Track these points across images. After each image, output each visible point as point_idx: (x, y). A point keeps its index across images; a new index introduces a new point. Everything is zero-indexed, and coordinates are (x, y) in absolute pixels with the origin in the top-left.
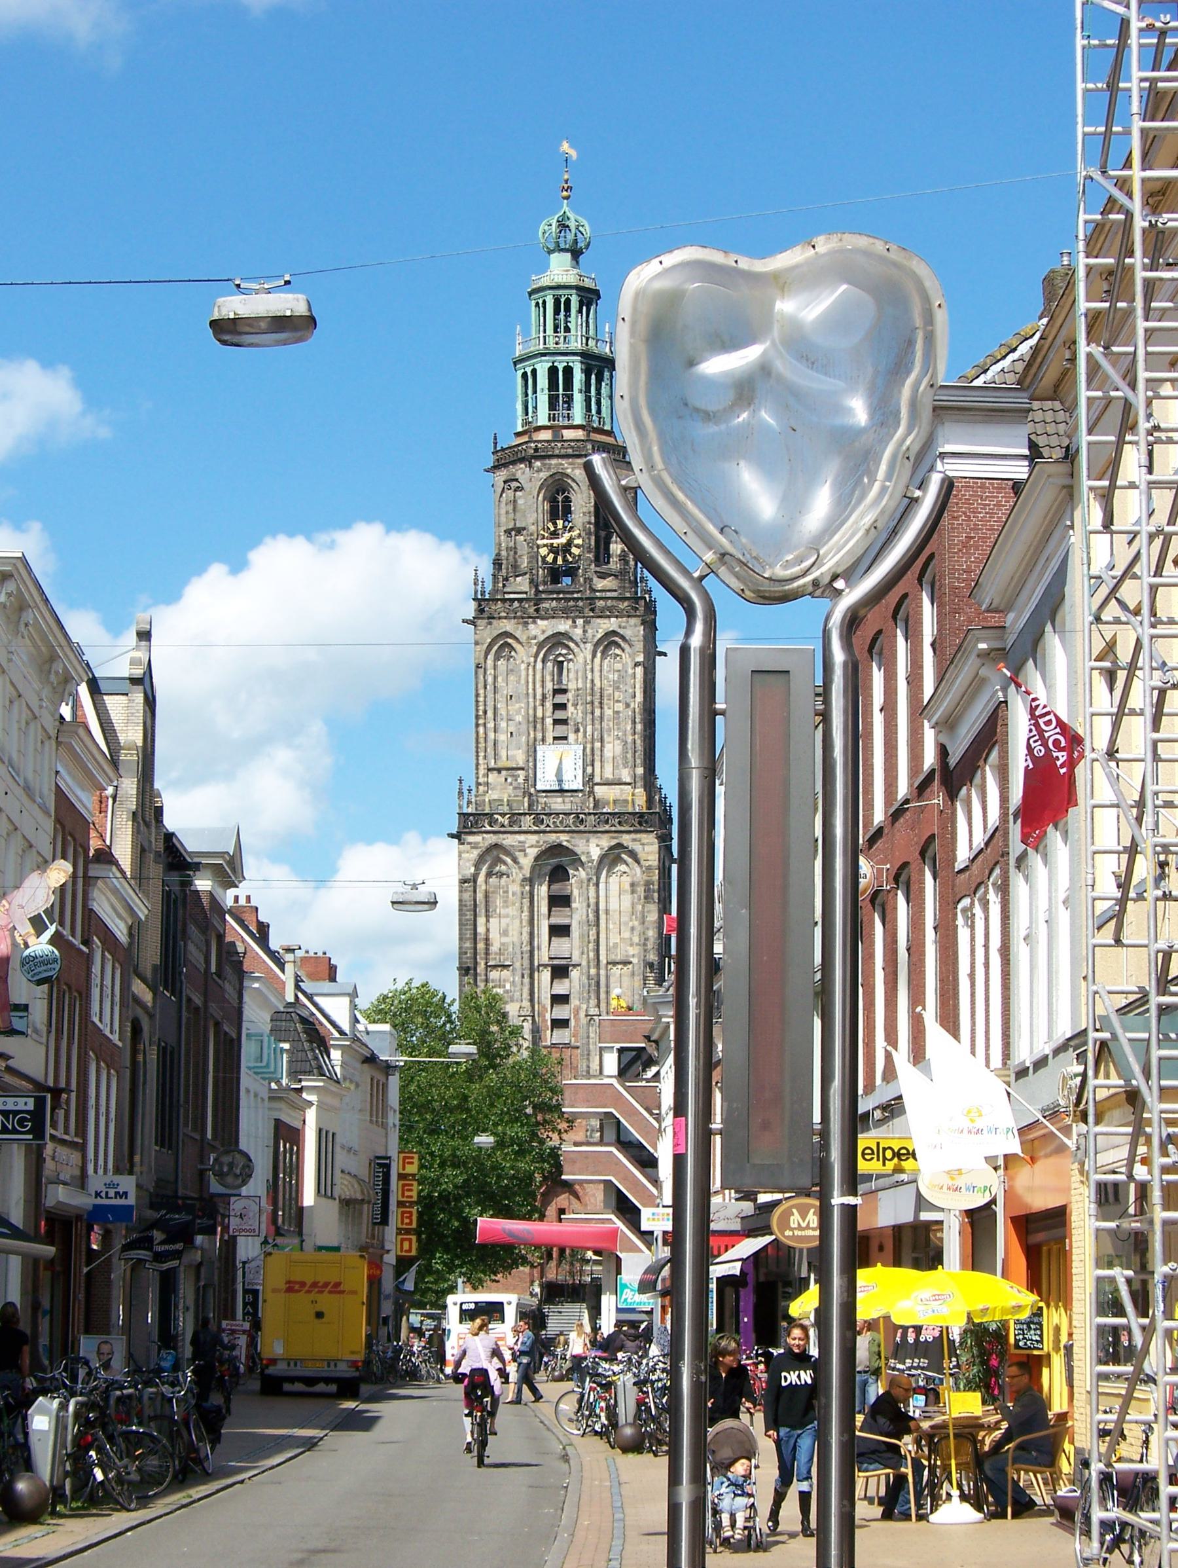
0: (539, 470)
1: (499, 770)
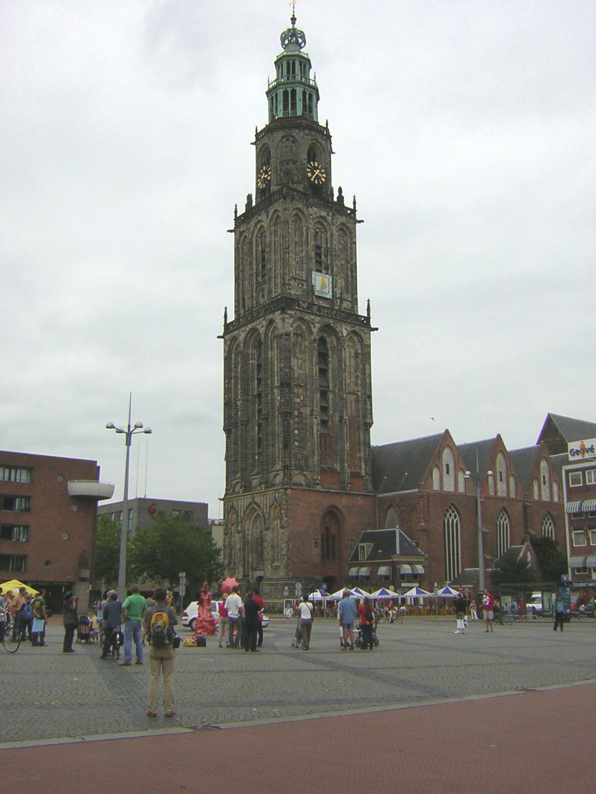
0: (307, 135)
1: (295, 279)
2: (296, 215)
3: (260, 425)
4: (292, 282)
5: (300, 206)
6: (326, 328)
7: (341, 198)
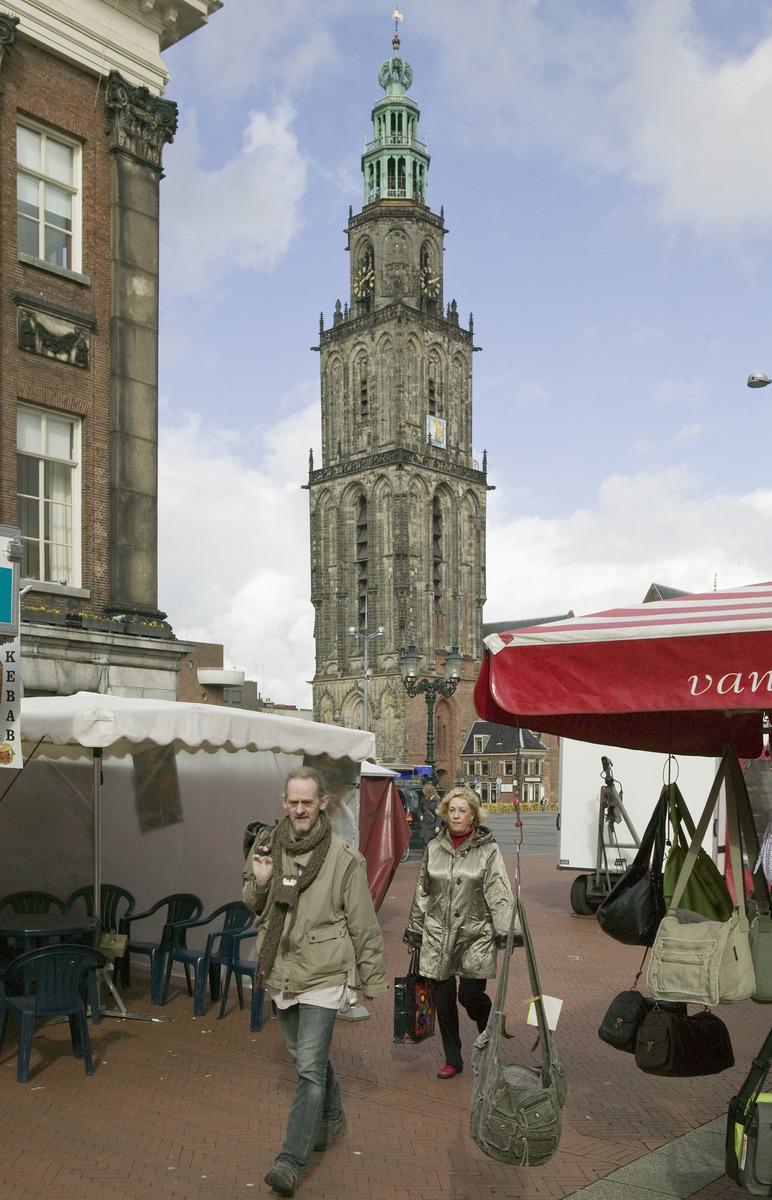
0: (421, 229)
1: (409, 425)
2: (410, 341)
3: (362, 599)
4: (407, 429)
5: (415, 330)
6: (443, 486)
7: (454, 315)
